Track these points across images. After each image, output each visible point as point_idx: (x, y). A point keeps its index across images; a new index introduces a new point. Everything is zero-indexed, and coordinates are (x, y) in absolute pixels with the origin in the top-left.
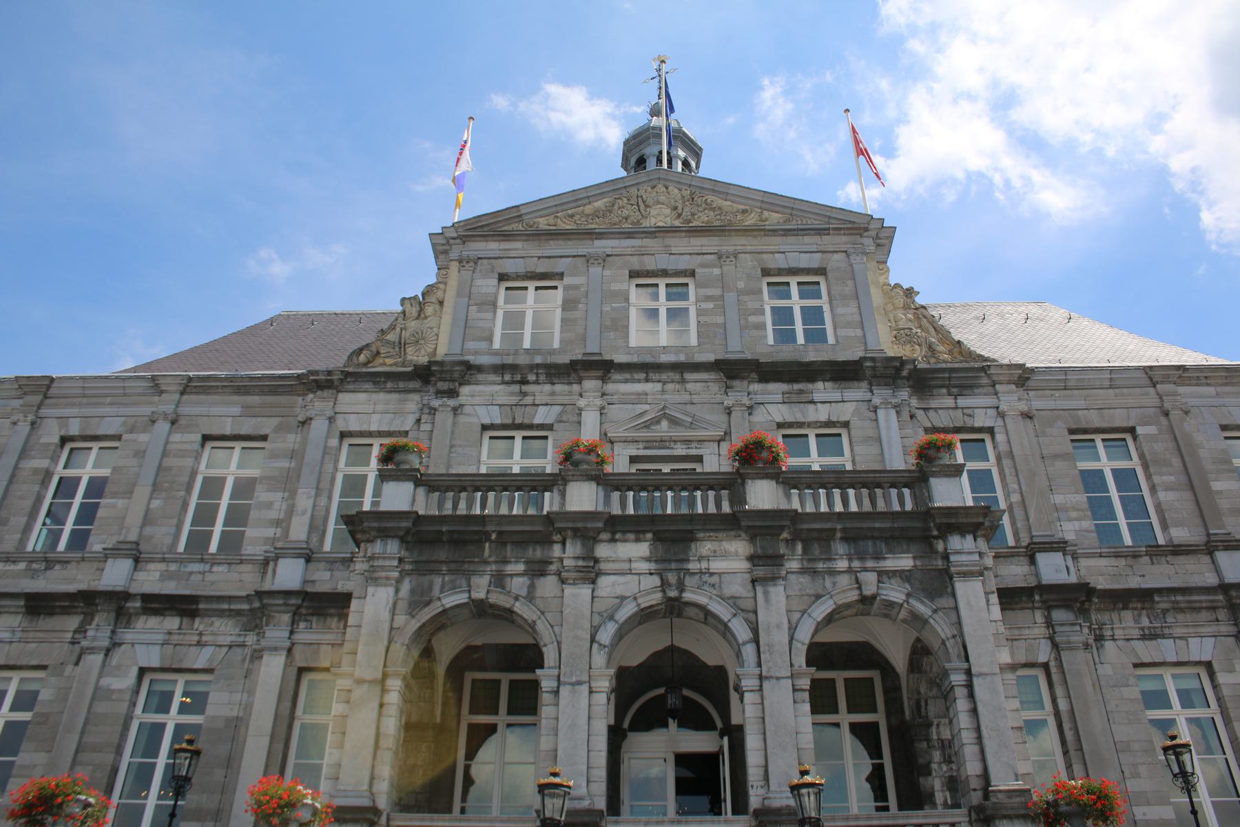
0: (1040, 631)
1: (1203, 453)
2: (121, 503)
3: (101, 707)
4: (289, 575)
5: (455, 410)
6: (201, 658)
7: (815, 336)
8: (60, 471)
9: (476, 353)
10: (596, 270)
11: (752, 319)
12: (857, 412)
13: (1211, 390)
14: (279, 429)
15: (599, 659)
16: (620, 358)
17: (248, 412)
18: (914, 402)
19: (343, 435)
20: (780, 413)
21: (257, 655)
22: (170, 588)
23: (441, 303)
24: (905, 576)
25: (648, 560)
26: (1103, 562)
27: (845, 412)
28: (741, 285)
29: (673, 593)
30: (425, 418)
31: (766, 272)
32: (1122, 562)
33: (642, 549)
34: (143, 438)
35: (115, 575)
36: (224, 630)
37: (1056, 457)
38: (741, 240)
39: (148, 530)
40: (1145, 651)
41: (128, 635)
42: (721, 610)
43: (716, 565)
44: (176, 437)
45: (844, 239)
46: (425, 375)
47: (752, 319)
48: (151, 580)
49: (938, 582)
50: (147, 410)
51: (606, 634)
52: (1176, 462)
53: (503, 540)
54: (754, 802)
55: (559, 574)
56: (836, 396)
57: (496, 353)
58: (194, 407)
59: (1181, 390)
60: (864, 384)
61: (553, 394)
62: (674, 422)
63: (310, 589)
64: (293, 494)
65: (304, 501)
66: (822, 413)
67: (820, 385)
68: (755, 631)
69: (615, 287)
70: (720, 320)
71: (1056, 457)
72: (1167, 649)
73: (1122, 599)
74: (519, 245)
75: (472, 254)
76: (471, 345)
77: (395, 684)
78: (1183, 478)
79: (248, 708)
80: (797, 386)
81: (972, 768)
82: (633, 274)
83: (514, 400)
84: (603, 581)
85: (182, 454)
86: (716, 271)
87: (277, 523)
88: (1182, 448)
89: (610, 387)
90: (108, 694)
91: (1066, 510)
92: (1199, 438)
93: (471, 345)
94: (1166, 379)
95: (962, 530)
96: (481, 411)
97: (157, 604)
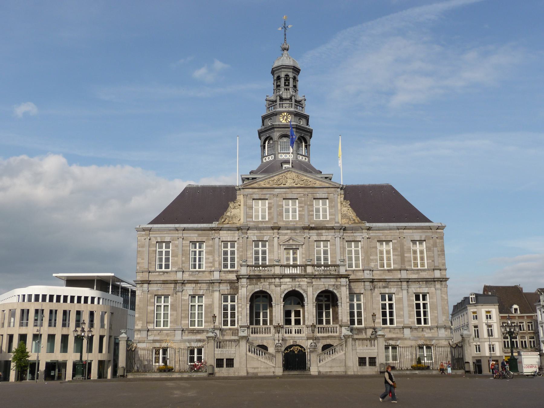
0: (362, 287)
1: (405, 247)
2: (176, 258)
3: (183, 303)
4: (216, 276)
5: (247, 238)
6: (201, 292)
7: (325, 216)
8: (158, 250)
9: (250, 222)
10: (275, 198)
11: (311, 213)
12: (332, 238)
13: (411, 231)
14: (207, 240)
15: (282, 300)
16: (281, 224)
17: (199, 235)
18: (345, 235)
19: (222, 241)
20: (315, 238)
21: (213, 291)
22: (192, 278)
23: (240, 205)
24: (334, 285)
25: (290, 282)
26: (378, 272)
27: (329, 238)
28: (308, 203)
29: (294, 289)
30: (241, 239)
31: (314, 199)
32: (382, 272)
33: (288, 280)
34: (177, 242)
35: (179, 276)
36: (204, 286)
37: (373, 248)
38: (309, 190)
39: (183, 265)
40: (383, 291)
41: (185, 288)
42: (302, 292)
43: (301, 283)
44: (184, 242)
45: (333, 189)
46: (238, 229)
47: (311, 213)
48: (186, 277)
49: (337, 287)
50: (177, 235)
51: (283, 296)
52: (399, 249)
53: (264, 278)
54: (306, 324)
55: (275, 285)
56: (328, 234)
57: (254, 222)
58: (186, 234)
59: (405, 231)
60: (333, 231)
61: (267, 233)
62: (293, 240)
63: (221, 278)
64: (213, 256)
65: (217, 259)
66: (324, 238)
67: (324, 231)
68: (307, 294)
69: (280, 203)
70: (303, 213)
71: (373, 248)
72: (387, 290)
73: (380, 281)
74: (256, 190)
75: (246, 193)
76: (248, 219)
77: (248, 305)
78: (399, 253)
79: (213, 302)
80: (320, 231)
81: (340, 318)
82: (284, 199)
83: (259, 234)
84: (282, 286)
85: (186, 246)
86: (303, 199)
87: (211, 263)
88: (402, 246)
89: (280, 231)
90: (184, 300)
91: (373, 260)
92: (405, 243)
93: (248, 219)
94: (401, 229)
95: (344, 277)
96: (252, 237)
97: (190, 282)
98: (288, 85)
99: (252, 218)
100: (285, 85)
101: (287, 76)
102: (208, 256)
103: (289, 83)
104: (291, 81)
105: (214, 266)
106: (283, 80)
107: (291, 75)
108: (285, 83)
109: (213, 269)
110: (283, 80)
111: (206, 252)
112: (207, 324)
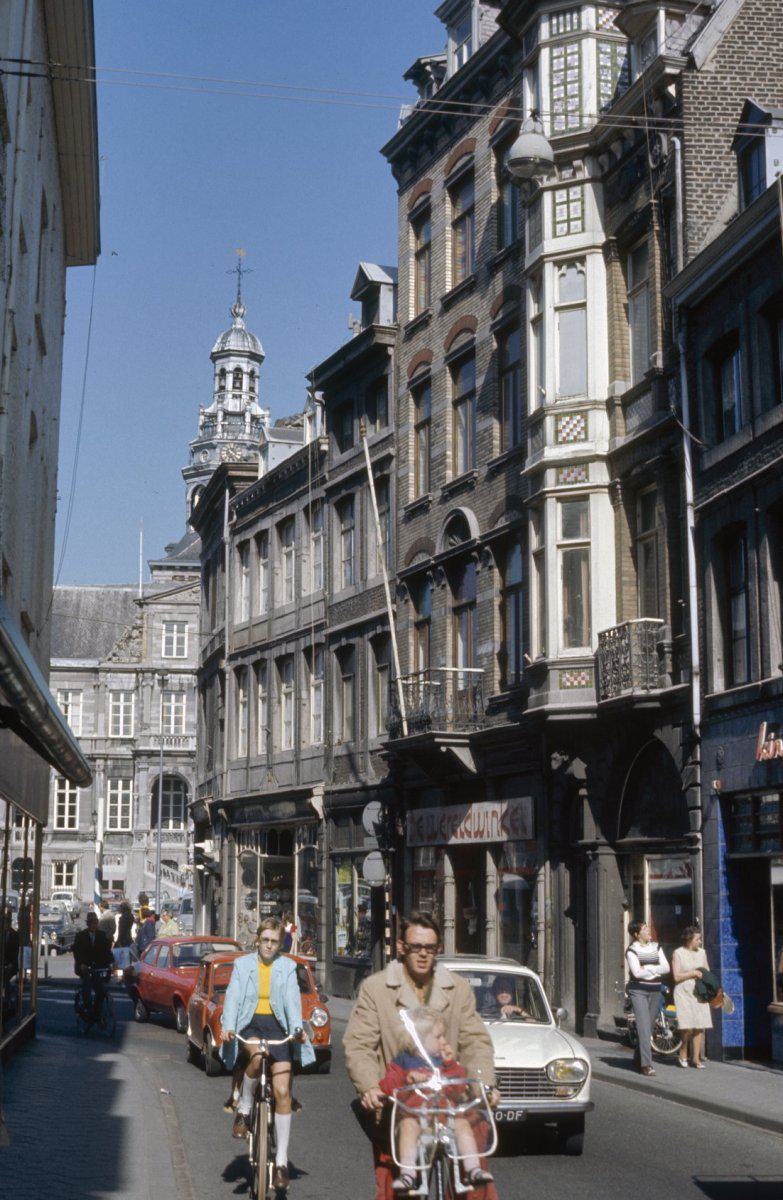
30: (140, 688)
98: (240, 388)
99: (160, 652)
100: (234, 387)
101: (238, 370)
102: (86, 715)
103: (241, 384)
104: (246, 379)
105: (96, 731)
106: (230, 378)
107: (246, 367)
108: (234, 383)
109: (95, 736)
110: (230, 378)
111: (83, 707)
112: (83, 825)
